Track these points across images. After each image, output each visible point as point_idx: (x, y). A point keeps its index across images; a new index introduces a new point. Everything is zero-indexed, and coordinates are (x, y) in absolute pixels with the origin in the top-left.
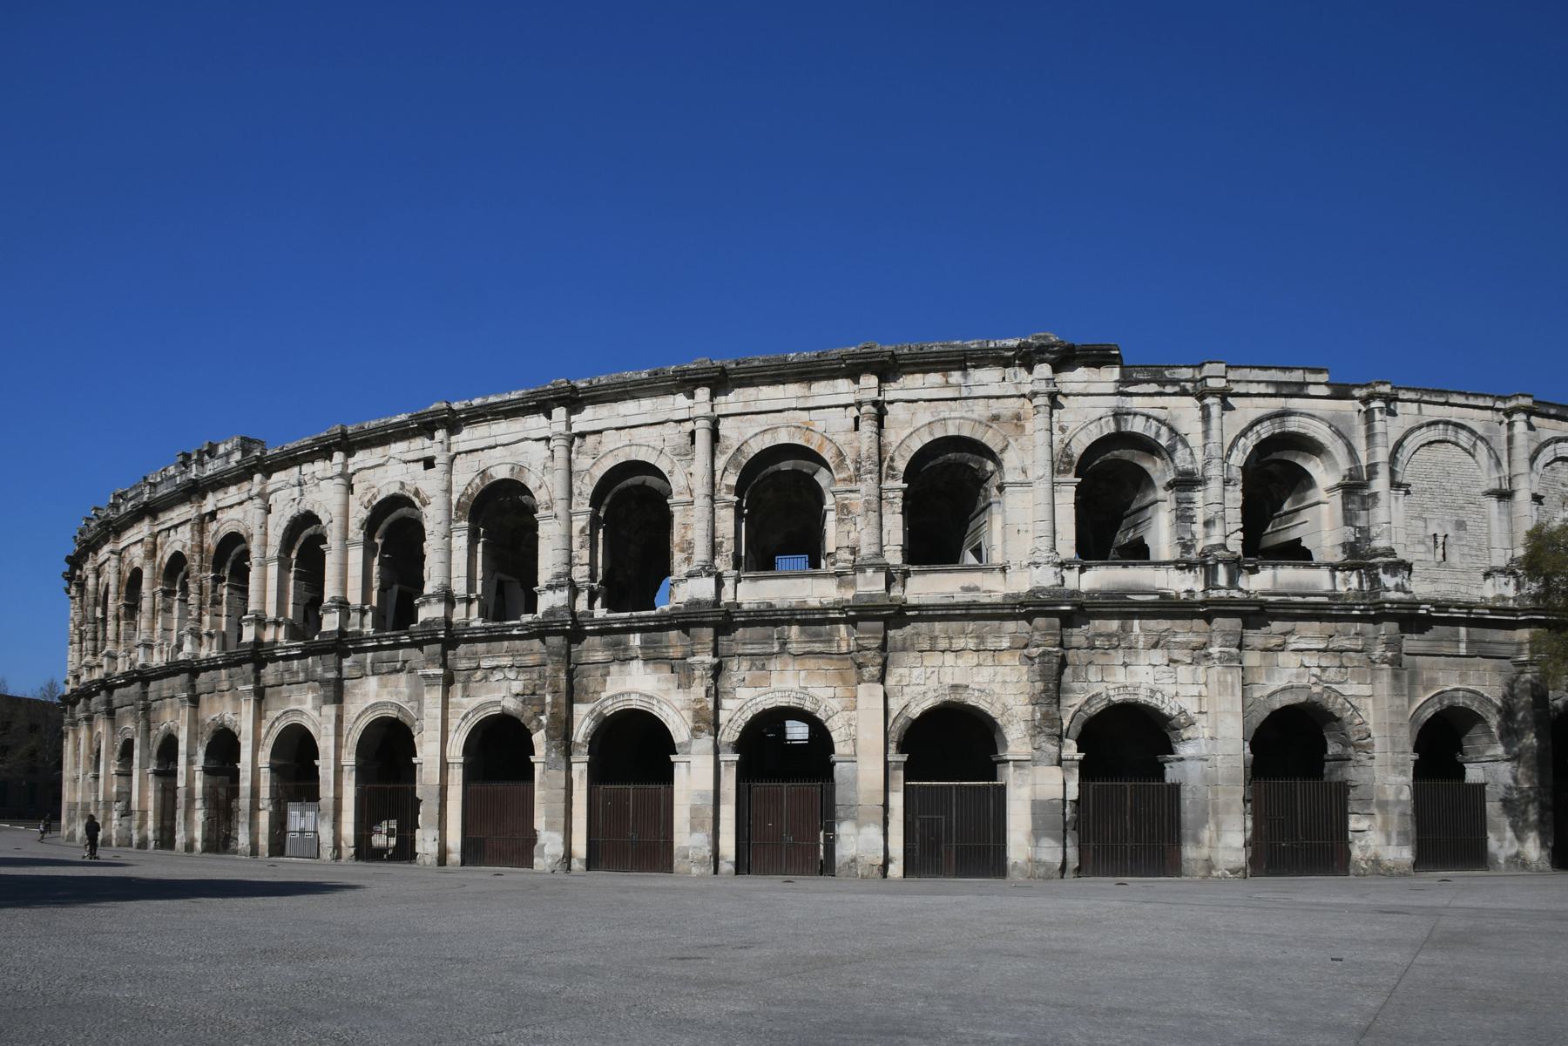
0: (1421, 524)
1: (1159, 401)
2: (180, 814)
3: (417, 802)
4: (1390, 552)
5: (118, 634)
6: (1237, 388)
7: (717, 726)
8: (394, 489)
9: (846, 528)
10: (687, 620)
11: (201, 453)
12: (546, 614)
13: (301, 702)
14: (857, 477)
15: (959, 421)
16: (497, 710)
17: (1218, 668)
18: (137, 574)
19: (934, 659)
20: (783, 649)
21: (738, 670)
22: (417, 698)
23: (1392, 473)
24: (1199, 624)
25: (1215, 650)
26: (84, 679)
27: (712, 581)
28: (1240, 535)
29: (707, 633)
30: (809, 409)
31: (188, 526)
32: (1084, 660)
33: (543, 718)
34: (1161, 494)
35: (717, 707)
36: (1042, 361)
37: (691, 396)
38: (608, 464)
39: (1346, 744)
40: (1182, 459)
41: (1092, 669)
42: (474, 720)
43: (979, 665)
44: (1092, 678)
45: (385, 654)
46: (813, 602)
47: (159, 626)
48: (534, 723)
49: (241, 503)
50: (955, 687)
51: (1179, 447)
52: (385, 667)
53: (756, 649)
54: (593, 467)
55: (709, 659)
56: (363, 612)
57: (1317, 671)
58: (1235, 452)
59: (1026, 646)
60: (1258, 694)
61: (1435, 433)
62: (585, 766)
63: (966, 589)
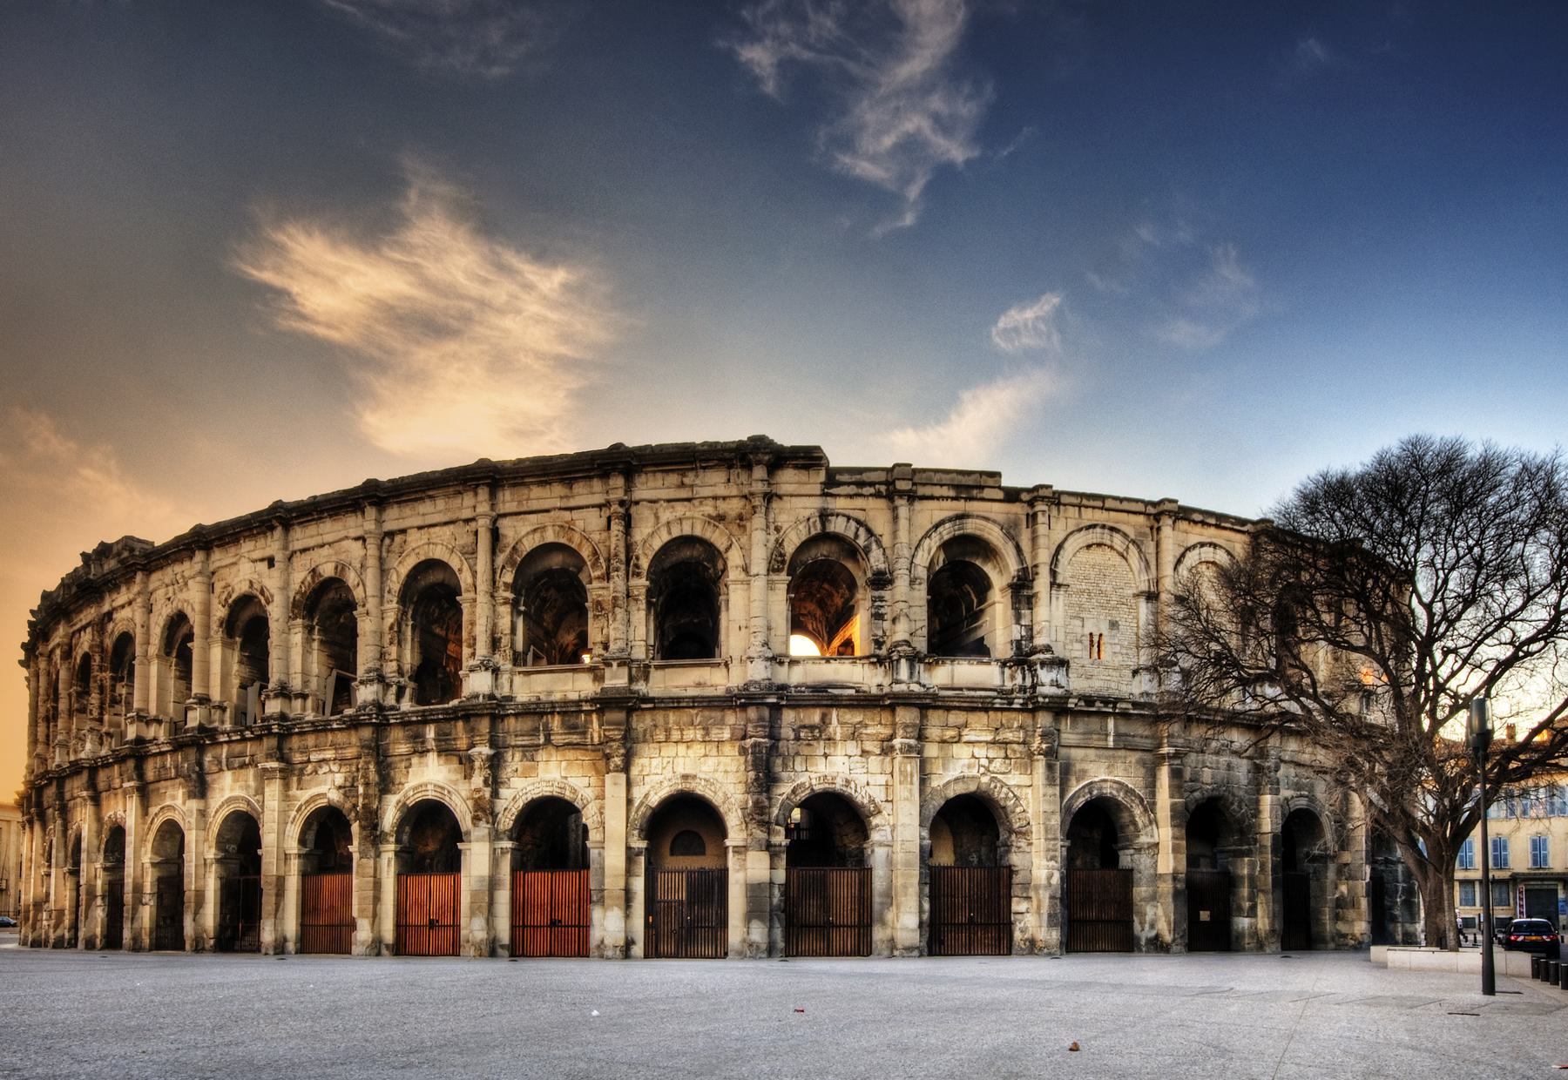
0: (1078, 623)
1: (859, 502)
4: (1048, 649)
6: (921, 491)
7: (494, 815)
10: (467, 714)
12: (359, 709)
13: (174, 798)
14: (607, 577)
15: (691, 521)
16: (322, 802)
17: (899, 758)
19: (669, 750)
20: (548, 741)
21: (514, 761)
22: (260, 791)
23: (1053, 573)
24: (886, 717)
25: (897, 742)
28: (925, 631)
29: (484, 725)
30: (571, 509)
32: (792, 752)
34: (859, 595)
35: (495, 794)
36: (759, 463)
37: (476, 494)
38: (411, 562)
39: (1011, 831)
40: (876, 560)
41: (798, 760)
42: (306, 812)
44: (798, 768)
45: (238, 748)
46: (573, 696)
50: (685, 777)
51: (874, 546)
53: (525, 741)
54: (401, 569)
55: (485, 750)
56: (224, 709)
57: (984, 762)
58: (920, 553)
59: (744, 738)
60: (936, 782)
61: (1095, 536)
62: (391, 855)
63: (699, 685)
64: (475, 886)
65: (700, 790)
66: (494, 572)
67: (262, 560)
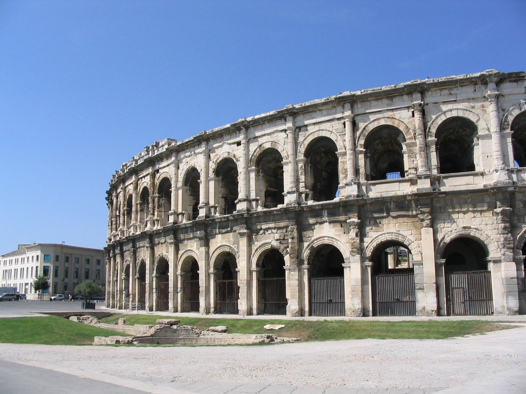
2: (147, 294)
3: (238, 288)
5: (124, 221)
8: (226, 155)
9: (412, 159)
11: (153, 146)
12: (288, 204)
13: (192, 246)
16: (269, 247)
18: (131, 196)
22: (237, 243)
26: (113, 240)
27: (355, 187)
31: (149, 176)
33: (288, 249)
35: (362, 241)
43: (474, 217)
46: (400, 193)
47: (139, 217)
48: (285, 252)
49: (168, 165)
50: (464, 228)
52: (224, 231)
56: (215, 208)
64: (353, 283)
65: (472, 234)
66: (354, 140)
67: (234, 143)
